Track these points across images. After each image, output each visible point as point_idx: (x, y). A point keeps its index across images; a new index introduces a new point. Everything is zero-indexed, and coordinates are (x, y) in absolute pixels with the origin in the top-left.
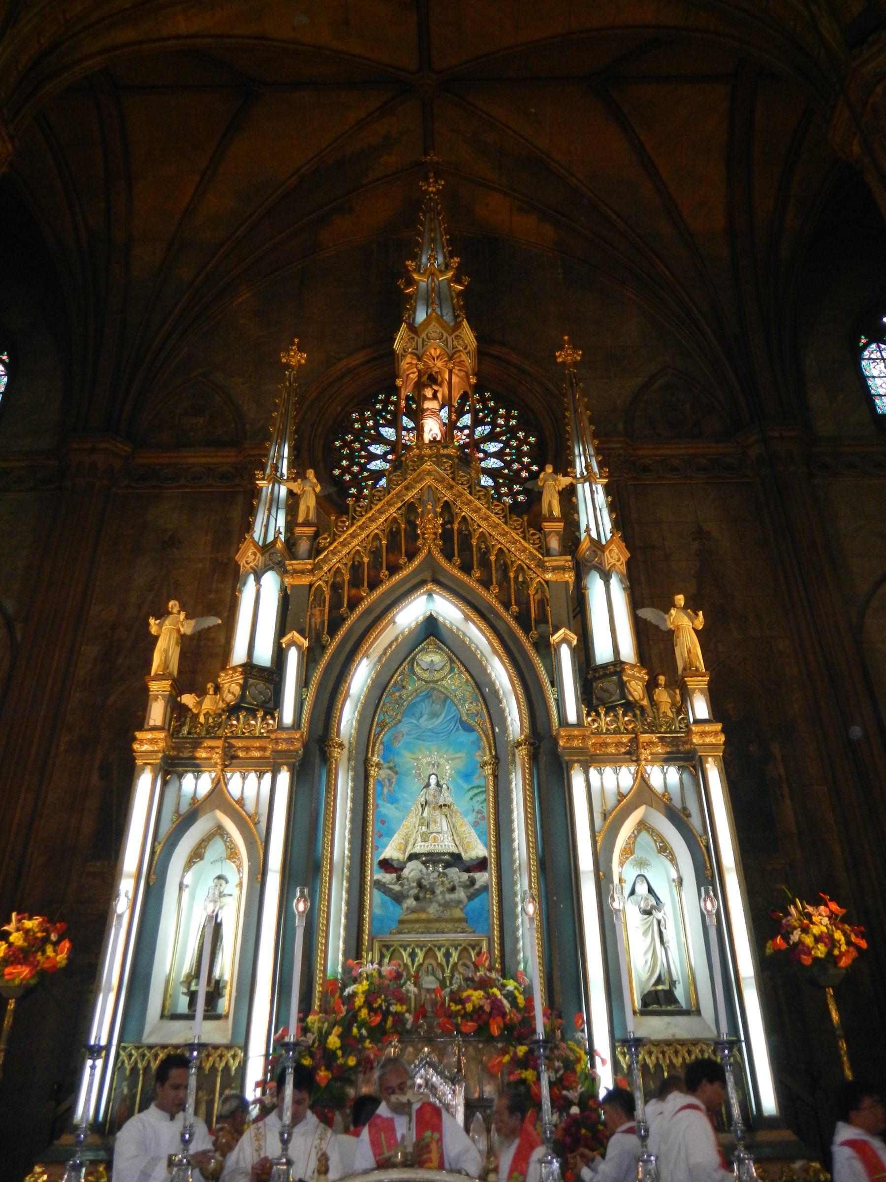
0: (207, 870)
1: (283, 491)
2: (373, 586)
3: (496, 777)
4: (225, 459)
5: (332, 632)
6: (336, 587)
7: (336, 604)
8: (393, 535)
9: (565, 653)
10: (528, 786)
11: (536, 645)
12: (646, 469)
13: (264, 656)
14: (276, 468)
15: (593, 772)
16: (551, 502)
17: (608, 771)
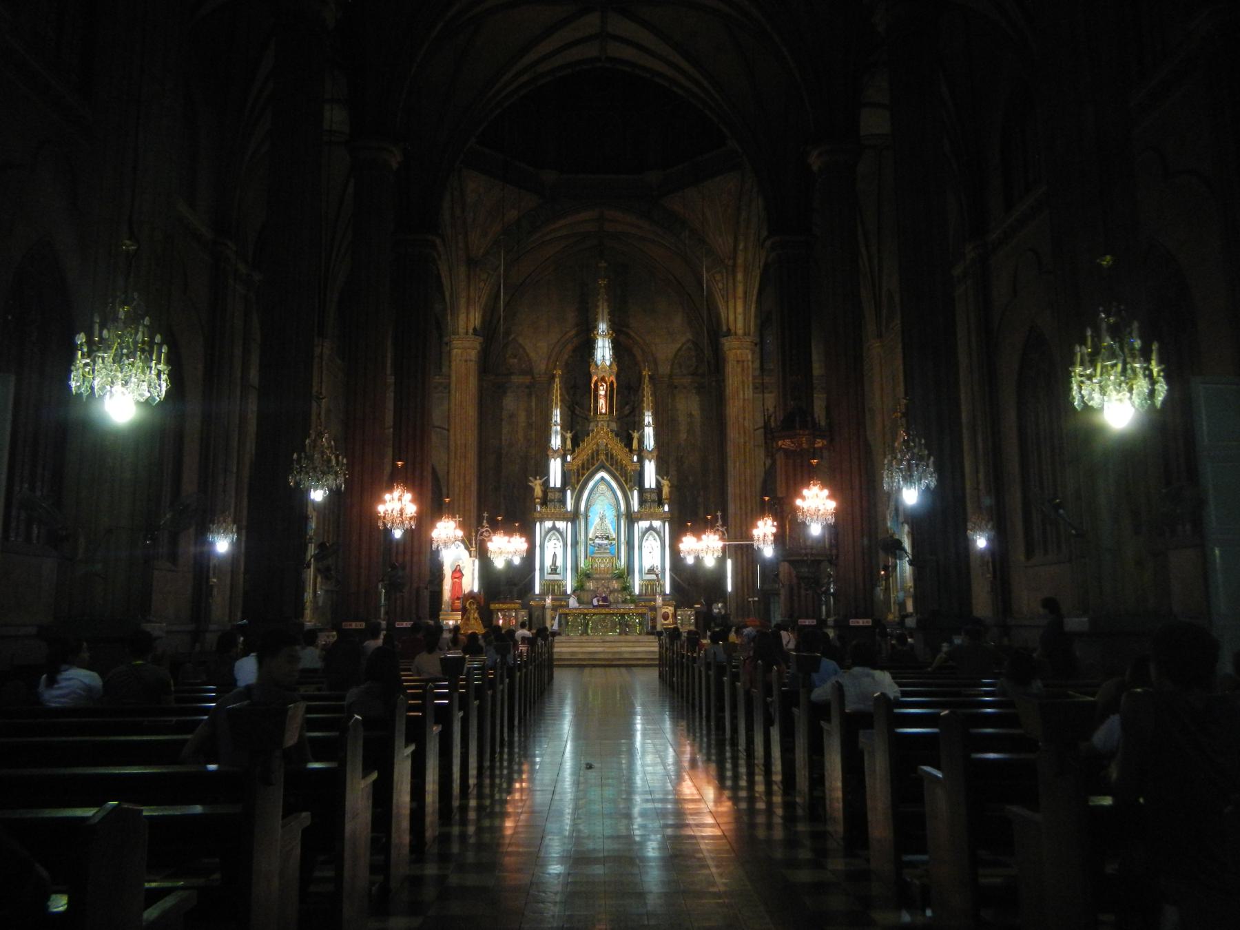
0: (553, 542)
1: (559, 428)
2: (588, 469)
3: (618, 519)
4: (527, 380)
5: (578, 483)
6: (578, 470)
7: (578, 476)
8: (593, 454)
9: (636, 493)
10: (625, 525)
11: (629, 489)
12: (676, 387)
13: (558, 485)
14: (556, 421)
15: (640, 522)
16: (635, 444)
17: (643, 522)
